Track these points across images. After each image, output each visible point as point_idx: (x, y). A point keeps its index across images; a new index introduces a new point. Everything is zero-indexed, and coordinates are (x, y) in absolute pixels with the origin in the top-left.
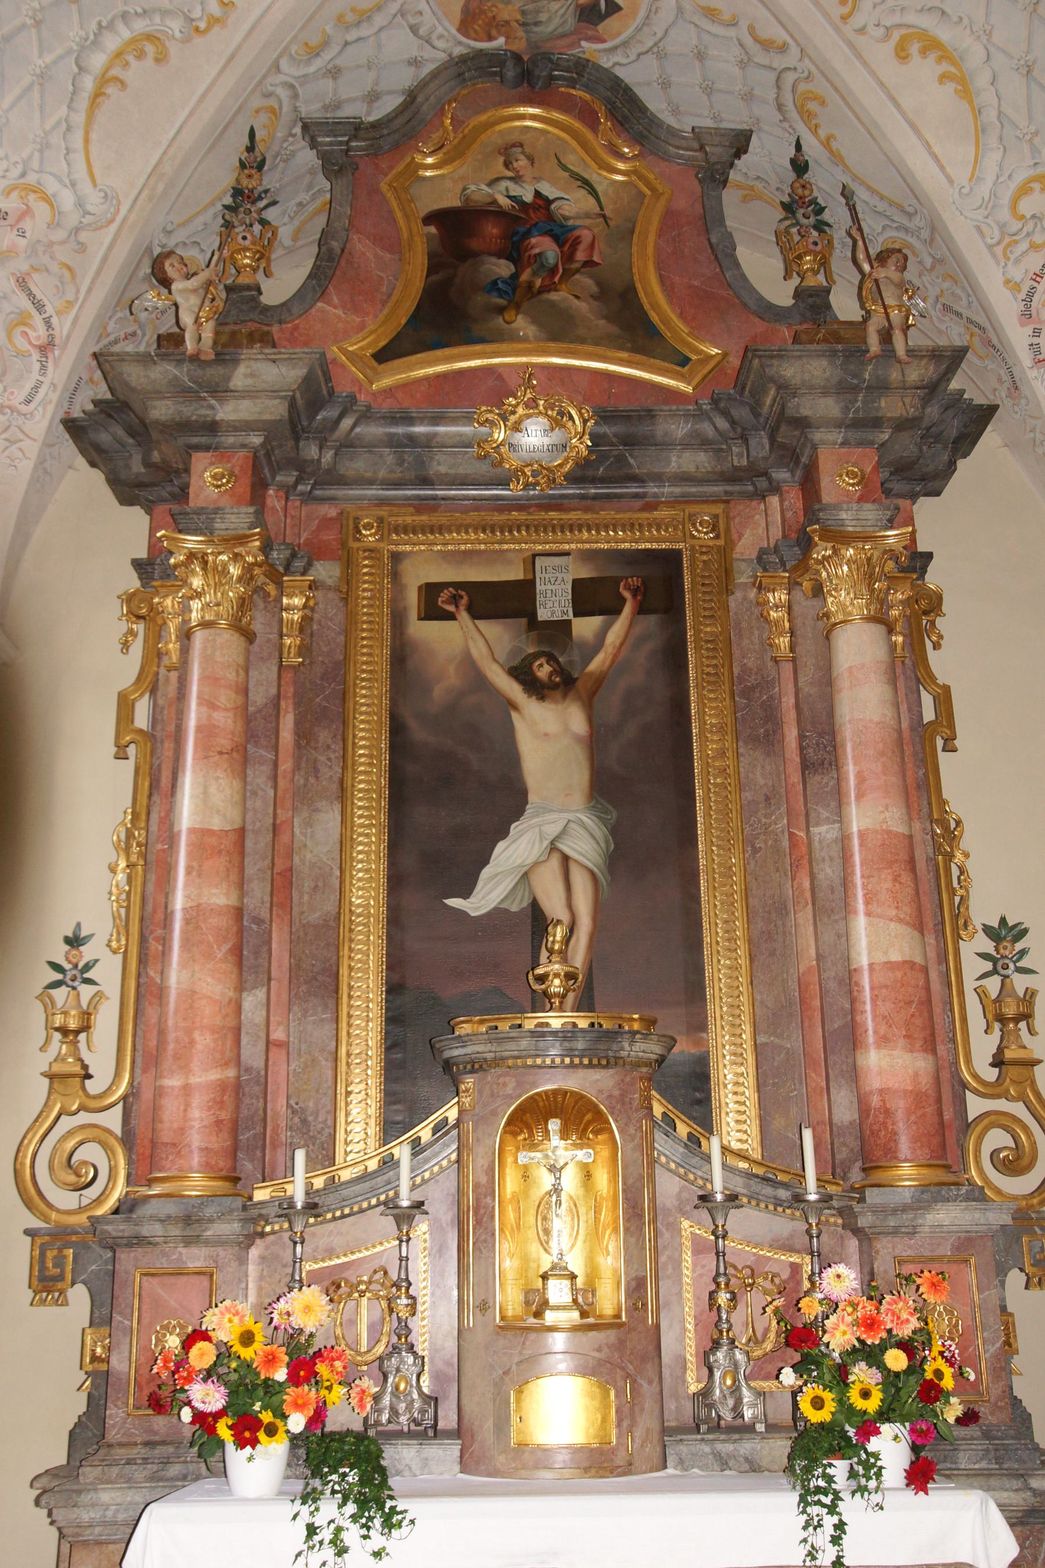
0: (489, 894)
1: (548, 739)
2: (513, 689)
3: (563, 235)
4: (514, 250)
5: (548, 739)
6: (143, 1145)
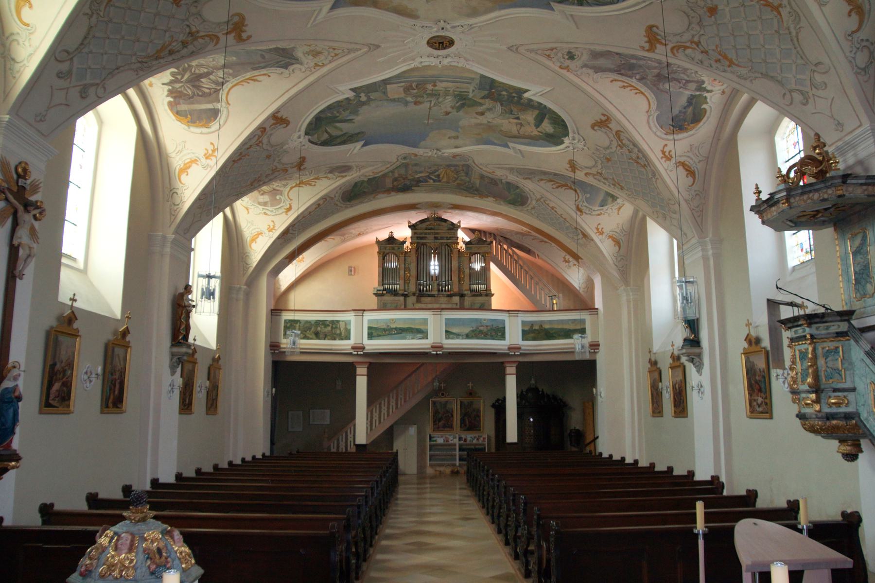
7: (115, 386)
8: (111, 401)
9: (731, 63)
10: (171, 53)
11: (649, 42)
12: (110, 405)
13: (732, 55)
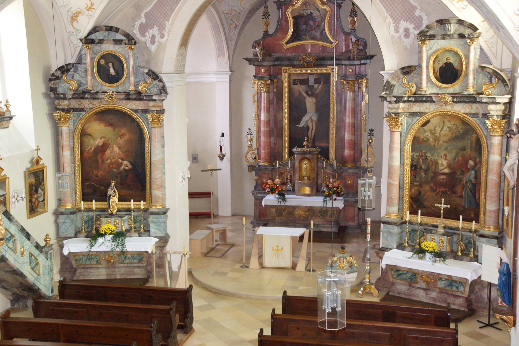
0: (302, 125)
2: (306, 95)
3: (314, 20)
4: (306, 24)
5: (310, 103)
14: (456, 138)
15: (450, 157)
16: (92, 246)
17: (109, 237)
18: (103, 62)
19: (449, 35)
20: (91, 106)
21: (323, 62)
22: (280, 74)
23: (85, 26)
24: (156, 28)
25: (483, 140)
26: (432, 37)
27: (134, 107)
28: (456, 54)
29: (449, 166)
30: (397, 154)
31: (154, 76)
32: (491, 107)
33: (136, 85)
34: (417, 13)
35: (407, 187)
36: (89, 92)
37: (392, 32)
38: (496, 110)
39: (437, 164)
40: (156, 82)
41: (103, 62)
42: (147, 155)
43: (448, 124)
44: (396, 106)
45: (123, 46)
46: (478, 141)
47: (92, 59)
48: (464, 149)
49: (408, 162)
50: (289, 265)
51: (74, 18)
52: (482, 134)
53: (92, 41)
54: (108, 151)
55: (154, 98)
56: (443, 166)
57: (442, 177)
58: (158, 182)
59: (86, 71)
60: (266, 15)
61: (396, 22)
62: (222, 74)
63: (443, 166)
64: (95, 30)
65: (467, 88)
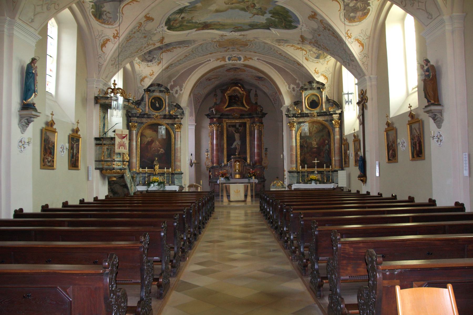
0: (233, 147)
1: (237, 136)
3: (238, 98)
5: (237, 136)
6: (213, 163)
7: (416, 145)
8: (415, 154)
9: (127, 41)
10: (334, 33)
11: (149, 17)
12: (415, 156)
13: (130, 41)
14: (320, 131)
15: (317, 140)
16: (149, 187)
17: (156, 184)
18: (153, 101)
19: (313, 88)
20: (146, 121)
21: (243, 117)
22: (222, 122)
23: (147, 83)
24: (178, 87)
25: (331, 131)
26: (306, 89)
27: (167, 122)
28: (317, 96)
29: (317, 144)
30: (294, 140)
31: (178, 107)
32: (334, 116)
33: (169, 112)
34: (297, 81)
35: (299, 156)
36: (147, 114)
37: (288, 89)
38: (336, 117)
39: (312, 144)
40: (179, 110)
41: (153, 101)
42: (173, 146)
43: (315, 126)
44: (293, 118)
45: (163, 93)
46: (329, 132)
47: (149, 99)
48: (323, 136)
49: (298, 144)
50: (242, 198)
51: (142, 80)
52: (330, 128)
53: (150, 91)
54: (153, 144)
55: (179, 117)
56: (314, 144)
57: (314, 149)
58: (179, 158)
59: (145, 105)
60: (215, 95)
61: (289, 85)
62: (192, 125)
63: (314, 144)
64: (151, 85)
65: (322, 109)
